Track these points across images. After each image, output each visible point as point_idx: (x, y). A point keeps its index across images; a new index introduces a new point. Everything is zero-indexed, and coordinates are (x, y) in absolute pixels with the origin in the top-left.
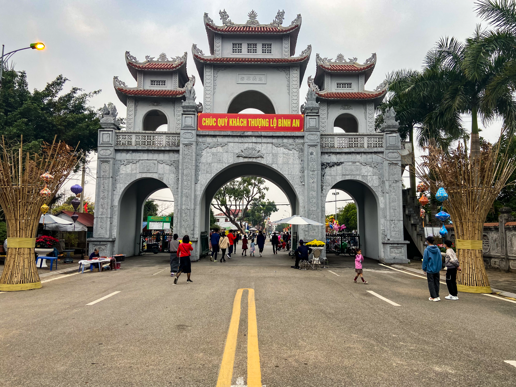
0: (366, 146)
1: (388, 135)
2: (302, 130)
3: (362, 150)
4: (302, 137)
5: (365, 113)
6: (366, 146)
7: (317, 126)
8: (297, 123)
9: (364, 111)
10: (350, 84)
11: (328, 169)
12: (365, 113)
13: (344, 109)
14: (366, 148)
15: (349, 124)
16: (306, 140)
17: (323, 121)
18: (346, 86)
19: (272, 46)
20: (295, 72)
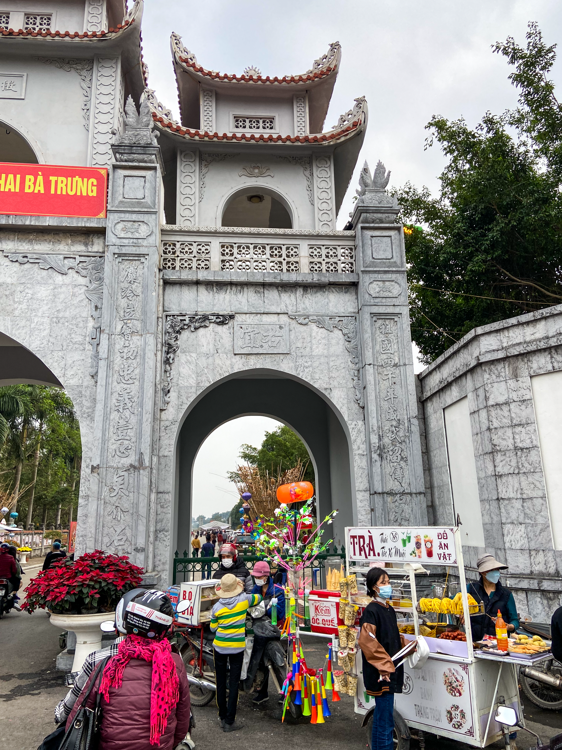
0: (305, 267)
1: (369, 233)
2: (102, 215)
3: (293, 277)
4: (101, 232)
5: (310, 189)
6: (305, 267)
7: (148, 200)
8: (86, 188)
9: (305, 183)
10: (272, 120)
11: (185, 334)
12: (310, 189)
13: (251, 175)
14: (304, 272)
15: (261, 211)
16: (110, 237)
17: (188, 202)
18: (261, 124)
19: (53, 18)
20: (106, 72)
